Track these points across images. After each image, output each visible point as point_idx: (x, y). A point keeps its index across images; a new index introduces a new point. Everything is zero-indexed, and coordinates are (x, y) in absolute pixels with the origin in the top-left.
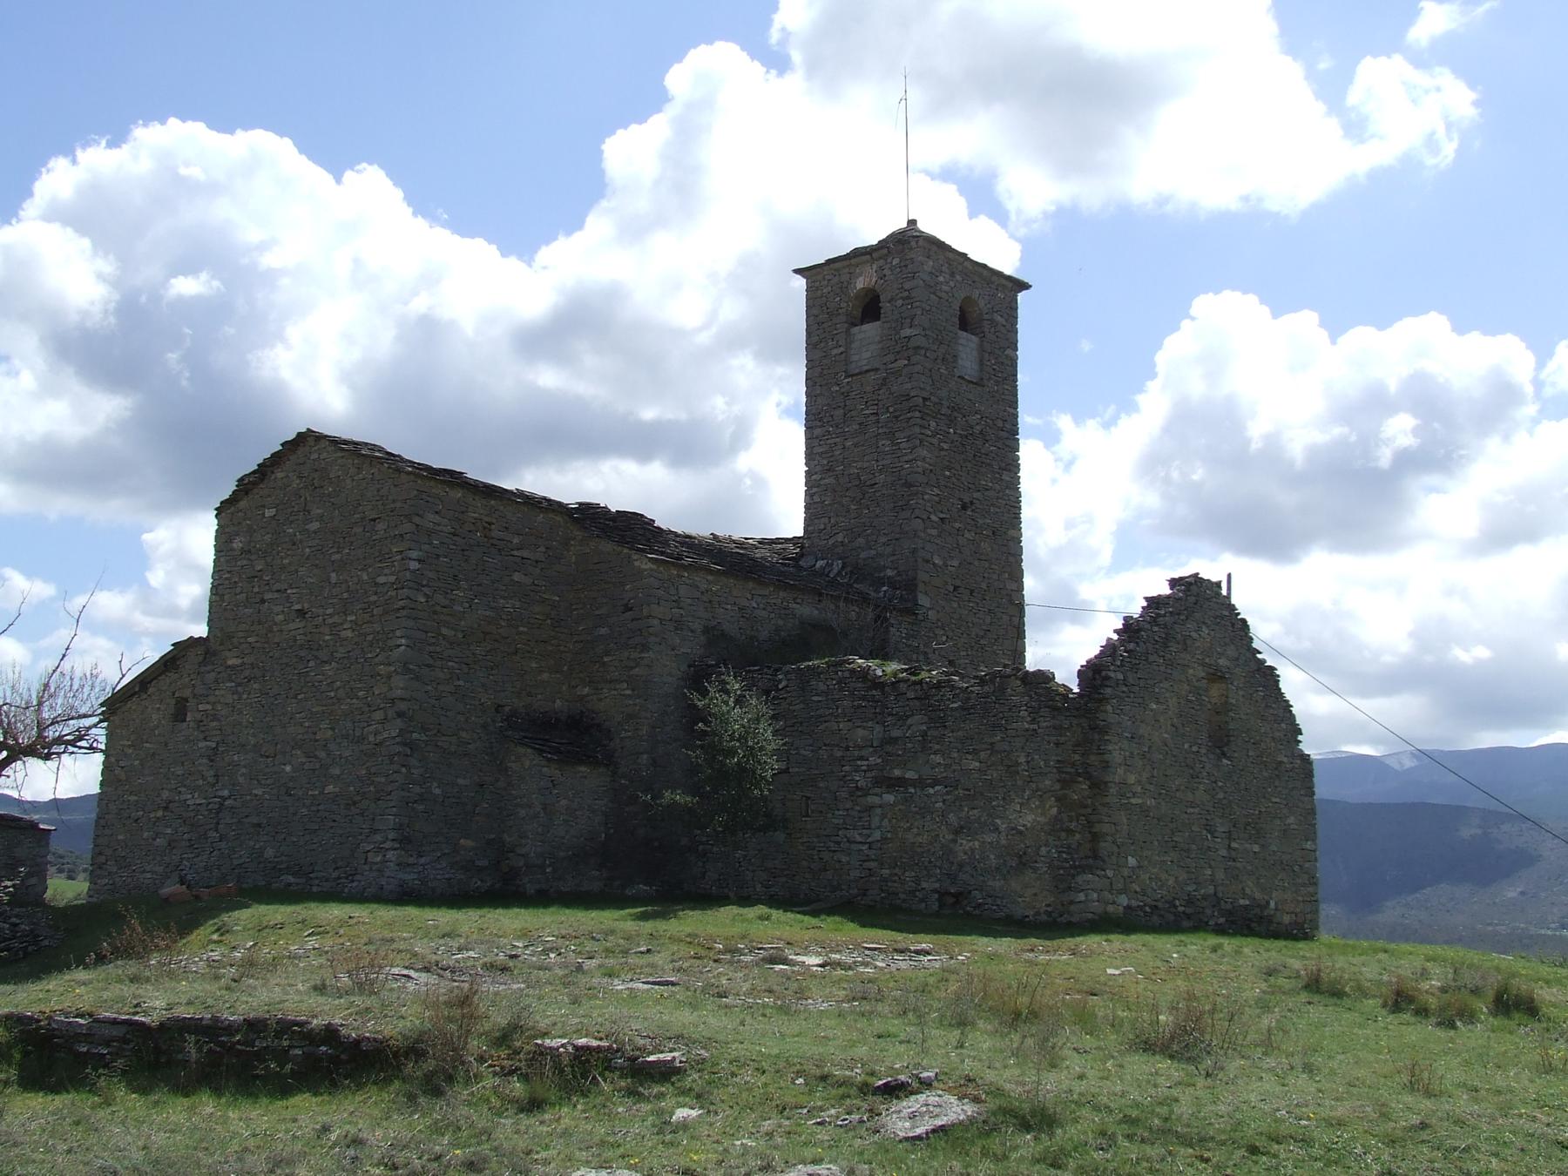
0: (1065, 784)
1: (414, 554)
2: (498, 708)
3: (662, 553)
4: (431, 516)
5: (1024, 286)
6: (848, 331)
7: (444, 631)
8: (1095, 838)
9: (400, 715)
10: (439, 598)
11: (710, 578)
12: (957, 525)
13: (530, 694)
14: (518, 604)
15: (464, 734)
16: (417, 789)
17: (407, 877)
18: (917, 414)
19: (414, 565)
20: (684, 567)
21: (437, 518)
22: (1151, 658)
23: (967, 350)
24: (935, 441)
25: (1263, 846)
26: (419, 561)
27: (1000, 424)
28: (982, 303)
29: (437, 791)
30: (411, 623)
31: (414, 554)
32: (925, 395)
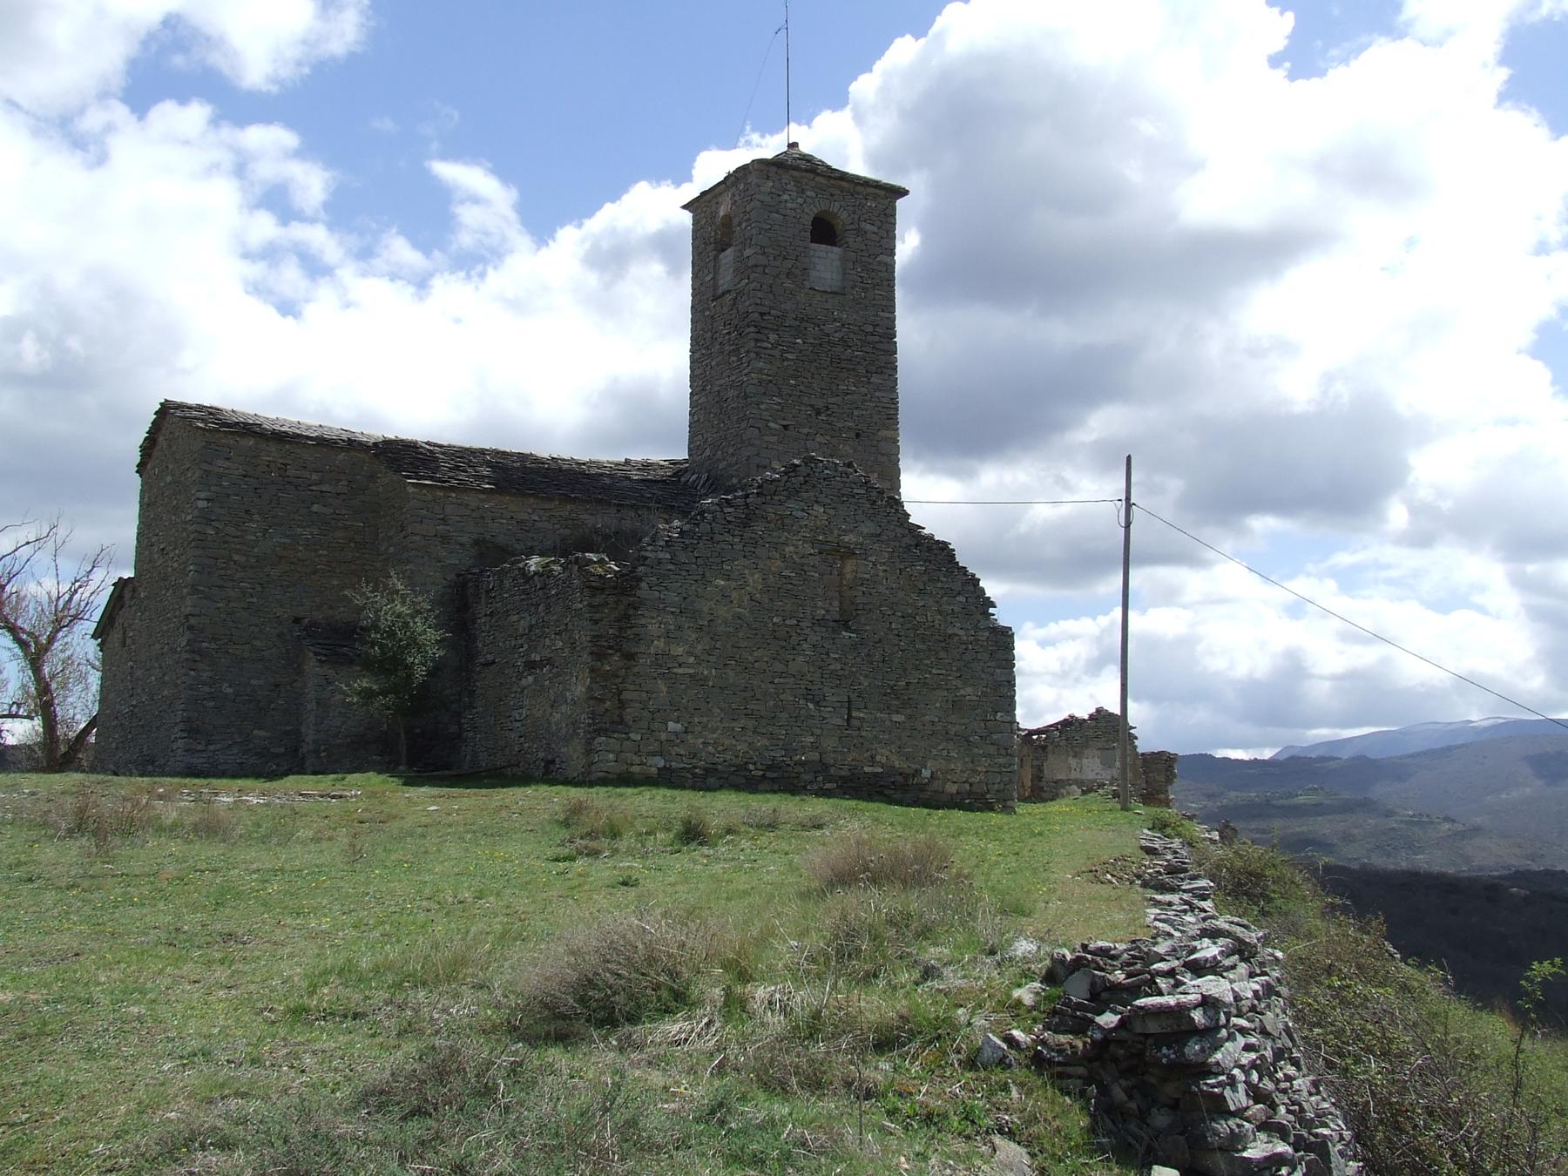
0: (599, 655)
1: (202, 495)
2: (297, 620)
3: (431, 478)
4: (220, 462)
5: (902, 192)
6: (716, 257)
7: (236, 557)
8: (622, 705)
9: (191, 628)
10: (231, 530)
11: (482, 496)
12: (805, 431)
13: (331, 607)
14: (316, 531)
15: (257, 643)
16: (207, 689)
17: (196, 761)
18: (752, 329)
19: (201, 504)
20: (452, 489)
21: (227, 464)
22: (717, 537)
23: (826, 265)
24: (776, 353)
25: (910, 717)
26: (208, 500)
27: (869, 329)
28: (844, 215)
29: (229, 690)
30: (199, 552)
31: (202, 495)
32: (766, 310)
